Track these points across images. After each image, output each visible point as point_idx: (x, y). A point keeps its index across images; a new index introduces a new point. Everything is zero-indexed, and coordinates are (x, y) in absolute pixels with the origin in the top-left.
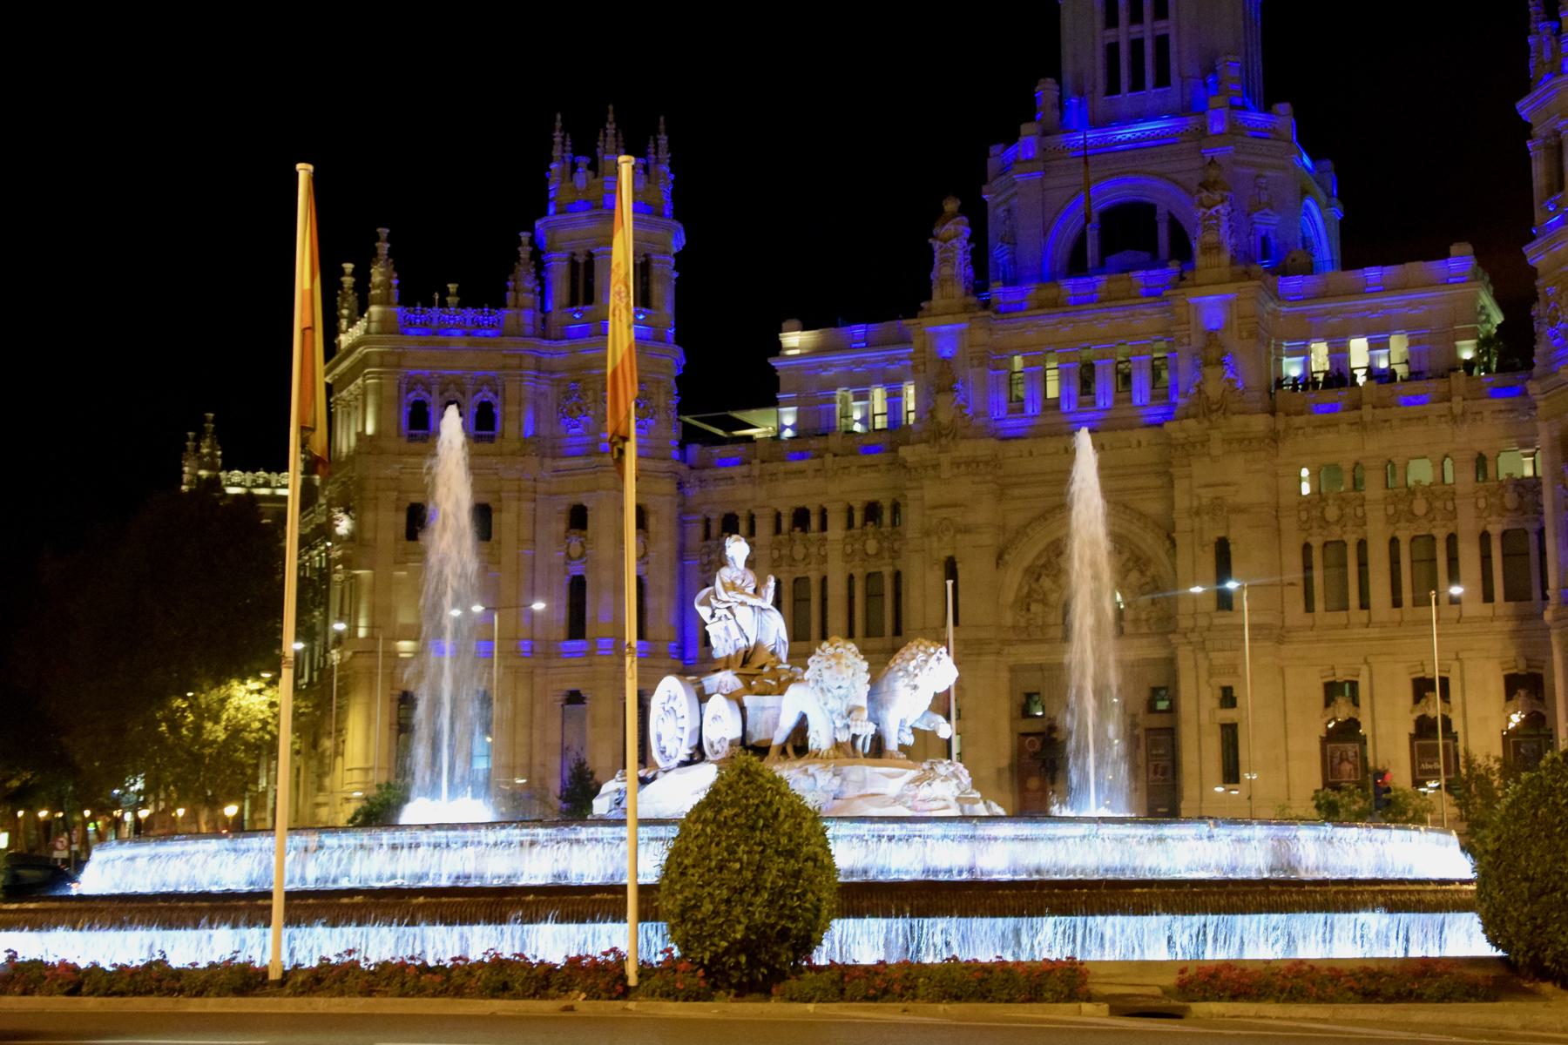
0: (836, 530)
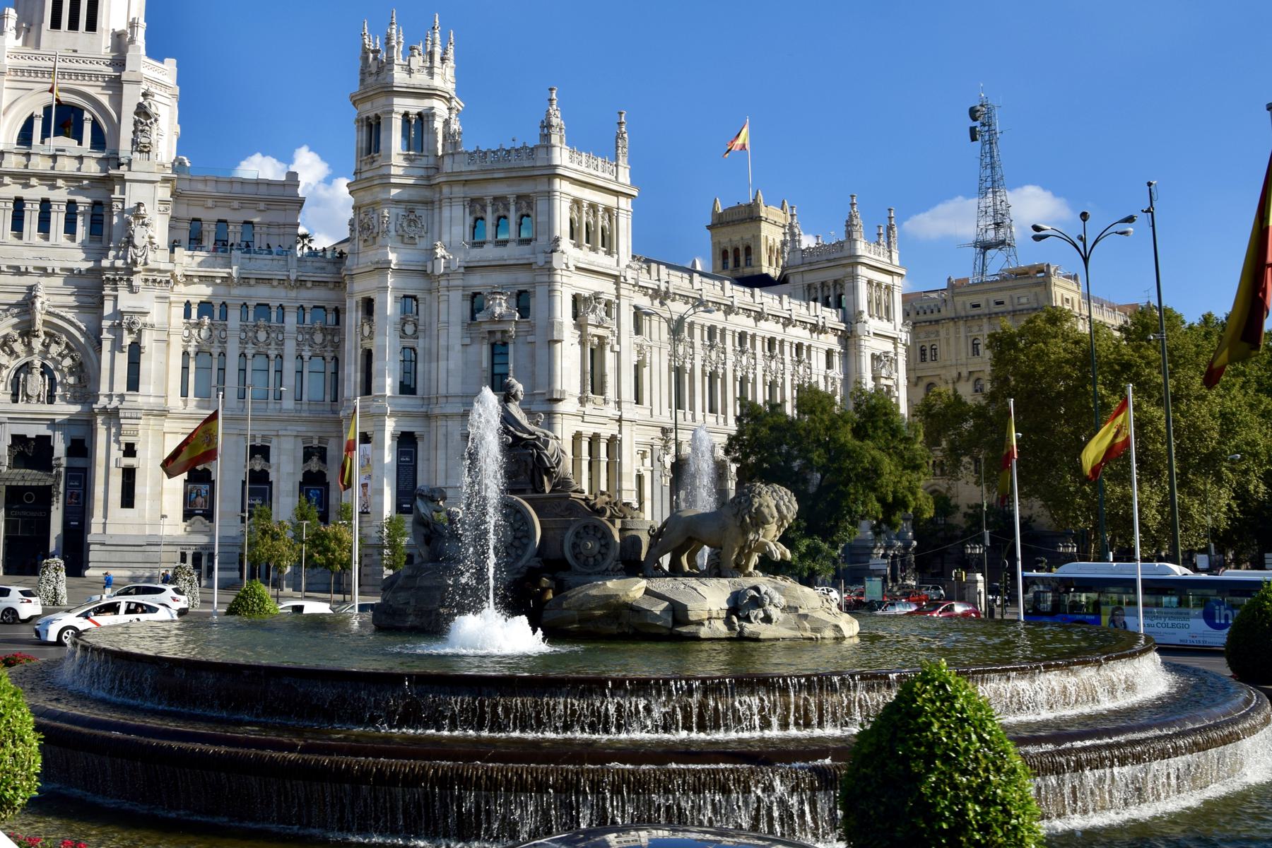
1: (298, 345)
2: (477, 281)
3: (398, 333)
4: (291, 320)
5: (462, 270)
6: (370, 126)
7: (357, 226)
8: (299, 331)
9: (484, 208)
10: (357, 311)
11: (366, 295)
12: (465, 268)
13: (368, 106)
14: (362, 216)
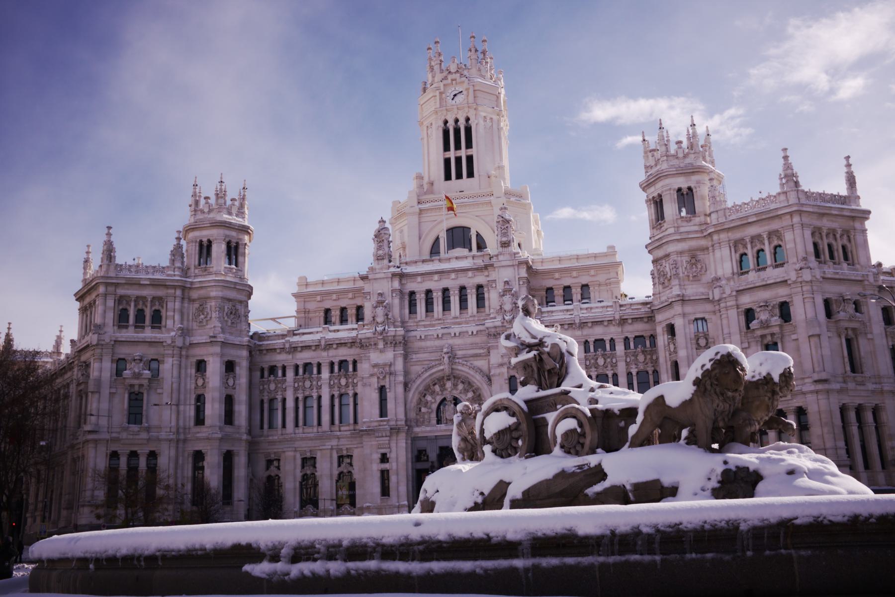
0: (325, 374)
1: (627, 364)
2: (747, 300)
3: (694, 346)
4: (620, 348)
5: (734, 293)
6: (656, 203)
7: (656, 275)
8: (626, 355)
9: (745, 246)
10: (663, 335)
11: (668, 322)
12: (737, 291)
13: (652, 189)
14: (659, 267)
